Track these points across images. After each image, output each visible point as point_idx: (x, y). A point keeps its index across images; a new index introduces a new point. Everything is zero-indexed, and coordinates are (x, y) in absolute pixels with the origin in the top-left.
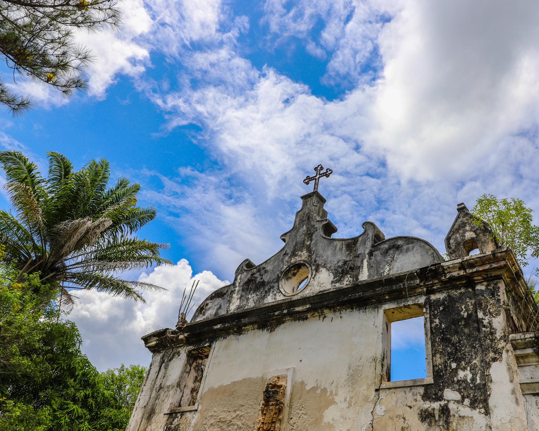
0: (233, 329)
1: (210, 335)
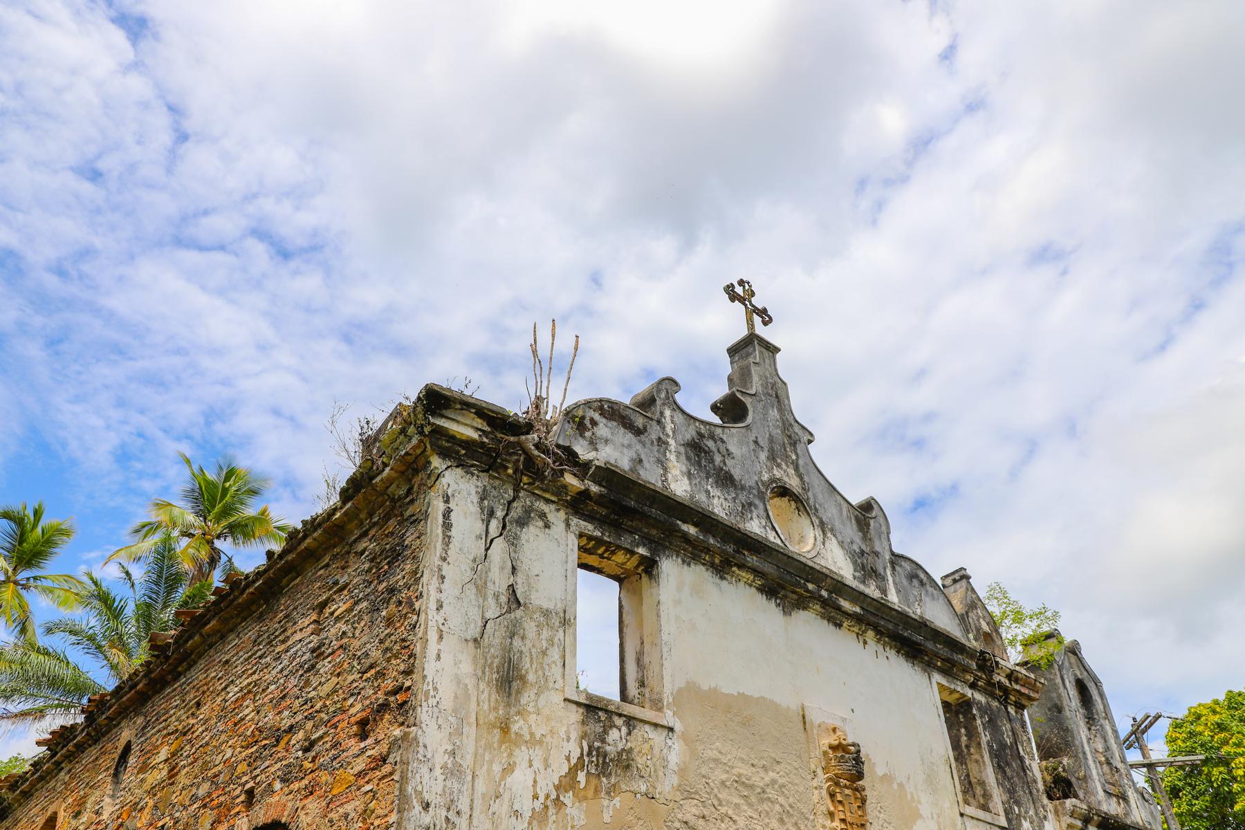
0: (712, 556)
1: (654, 532)
